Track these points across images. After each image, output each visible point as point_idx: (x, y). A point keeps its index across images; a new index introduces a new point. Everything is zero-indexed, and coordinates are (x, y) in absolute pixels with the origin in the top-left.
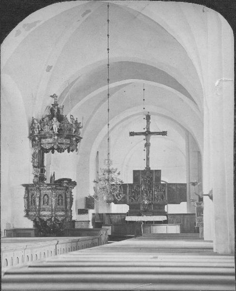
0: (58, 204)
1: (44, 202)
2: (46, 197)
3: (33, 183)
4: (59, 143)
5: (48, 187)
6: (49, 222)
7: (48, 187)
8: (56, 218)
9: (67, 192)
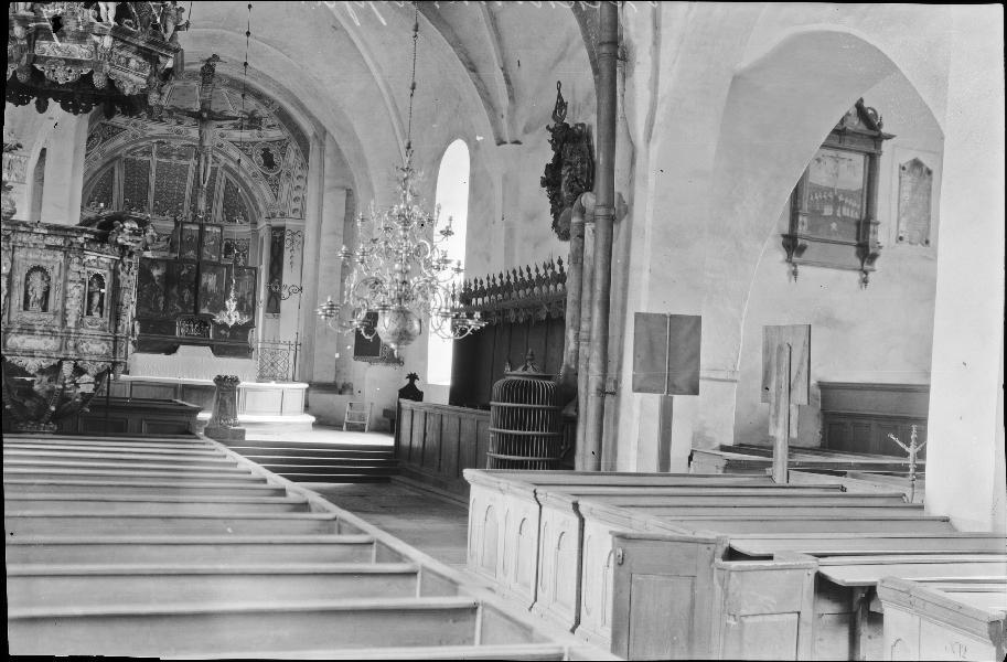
1: (27, 298)
2: (36, 279)
5: (50, 241)
6: (45, 379)
7: (50, 241)
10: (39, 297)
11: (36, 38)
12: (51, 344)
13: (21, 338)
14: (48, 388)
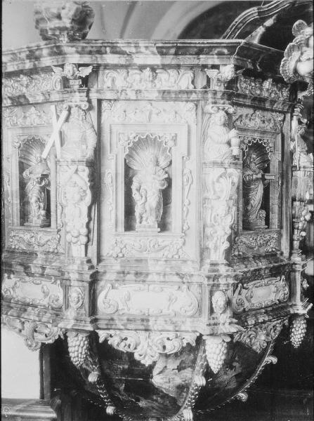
7: (168, 80)
14: (178, 381)
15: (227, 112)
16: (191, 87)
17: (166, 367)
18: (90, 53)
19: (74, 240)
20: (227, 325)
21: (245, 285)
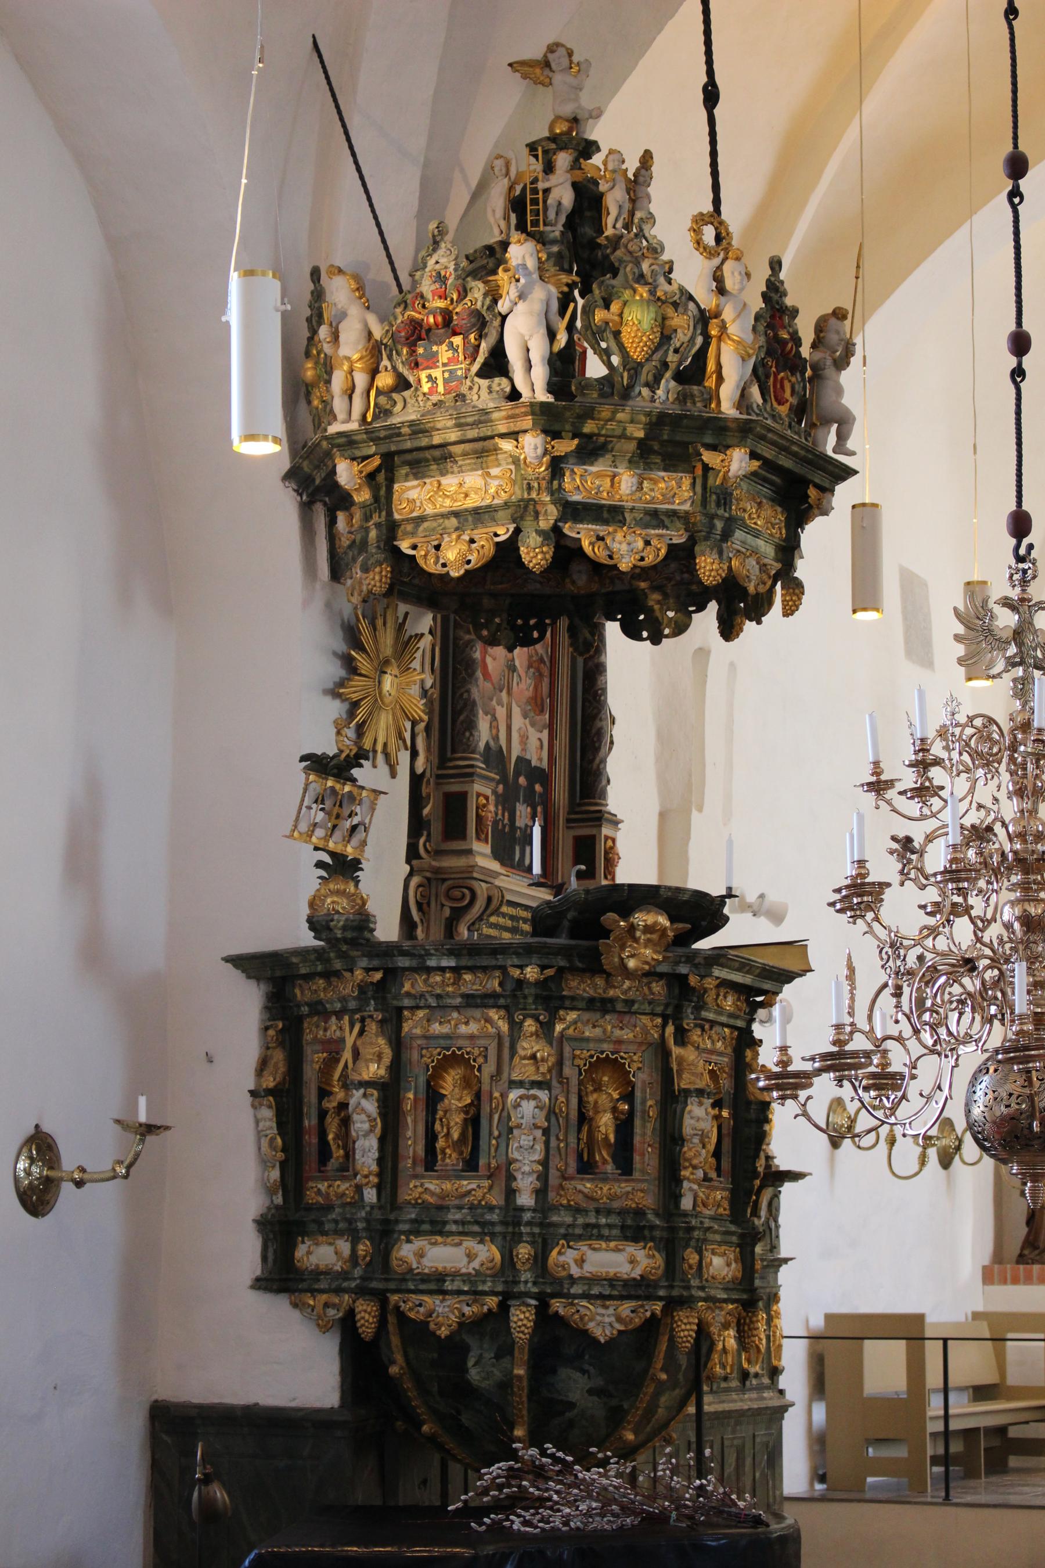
0: (586, 1167)
1: (431, 1138)
3: (307, 939)
4: (573, 511)
8: (557, 1306)
9: (681, 1036)
10: (456, 1135)
11: (391, 481)
12: (487, 1253)
13: (419, 1243)
14: (497, 1374)
15: (537, 1020)
16: (498, 989)
17: (481, 1355)
18: (378, 956)
19: (365, 1181)
20: (530, 1285)
21: (571, 1243)
